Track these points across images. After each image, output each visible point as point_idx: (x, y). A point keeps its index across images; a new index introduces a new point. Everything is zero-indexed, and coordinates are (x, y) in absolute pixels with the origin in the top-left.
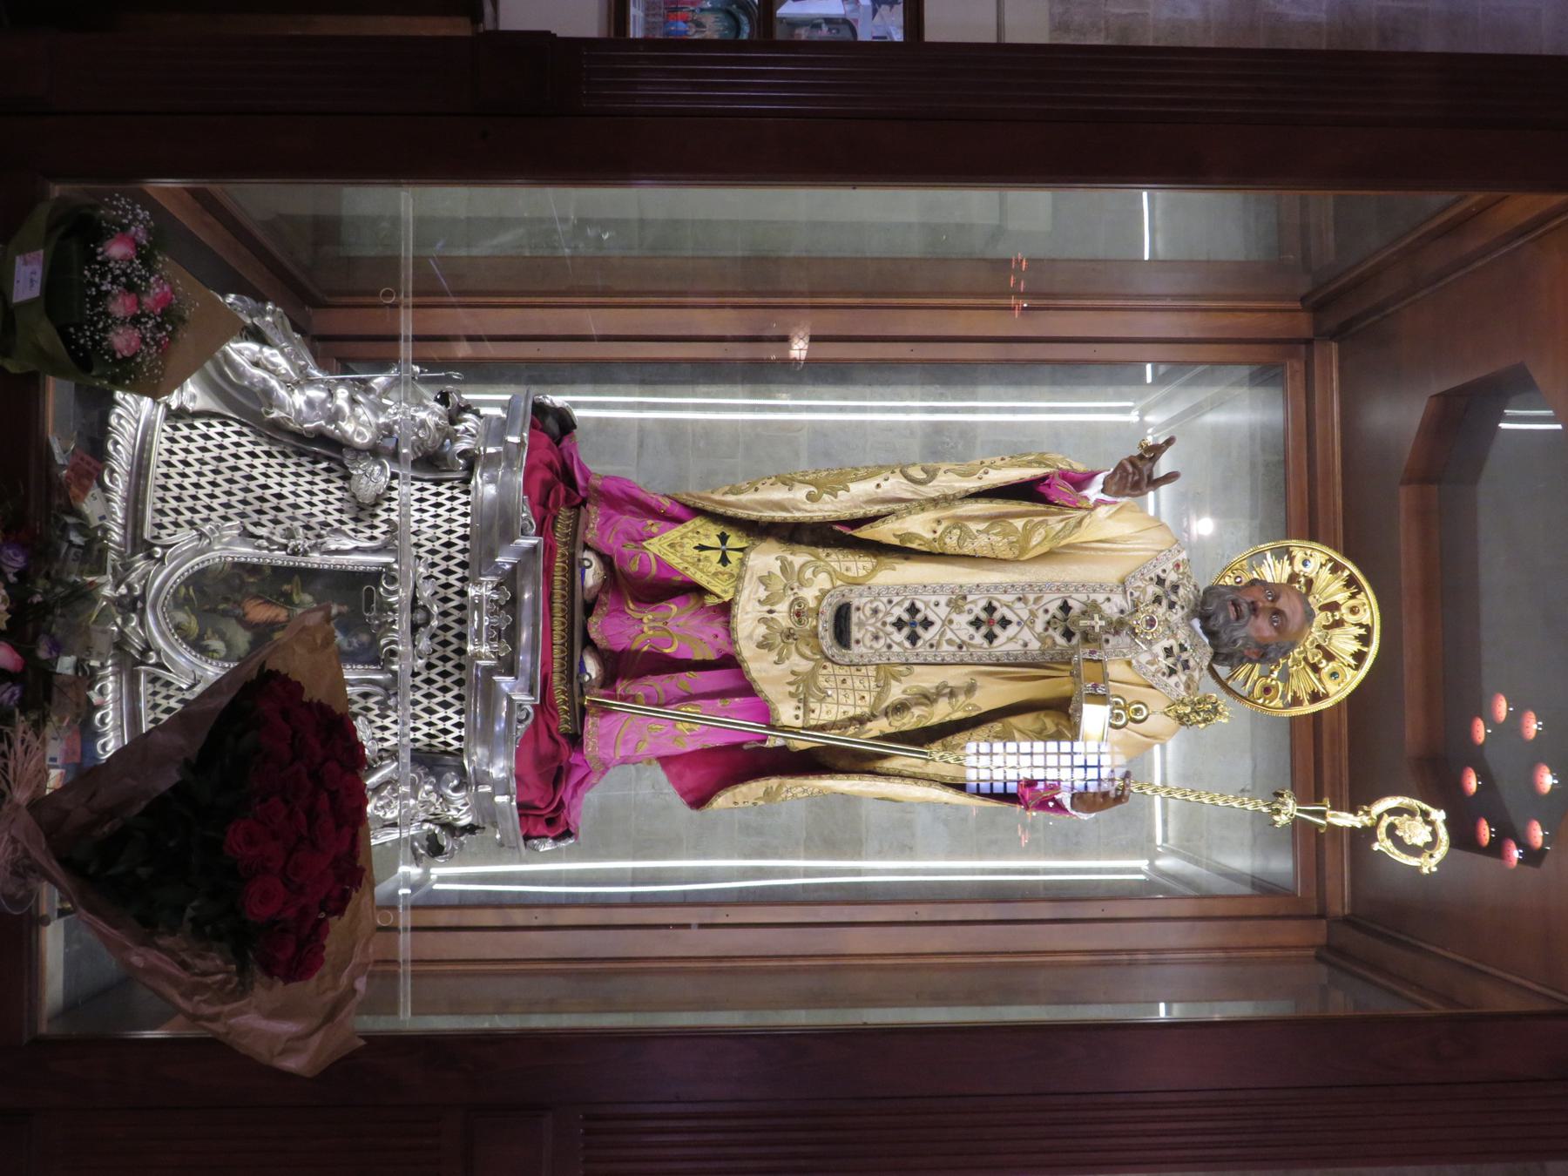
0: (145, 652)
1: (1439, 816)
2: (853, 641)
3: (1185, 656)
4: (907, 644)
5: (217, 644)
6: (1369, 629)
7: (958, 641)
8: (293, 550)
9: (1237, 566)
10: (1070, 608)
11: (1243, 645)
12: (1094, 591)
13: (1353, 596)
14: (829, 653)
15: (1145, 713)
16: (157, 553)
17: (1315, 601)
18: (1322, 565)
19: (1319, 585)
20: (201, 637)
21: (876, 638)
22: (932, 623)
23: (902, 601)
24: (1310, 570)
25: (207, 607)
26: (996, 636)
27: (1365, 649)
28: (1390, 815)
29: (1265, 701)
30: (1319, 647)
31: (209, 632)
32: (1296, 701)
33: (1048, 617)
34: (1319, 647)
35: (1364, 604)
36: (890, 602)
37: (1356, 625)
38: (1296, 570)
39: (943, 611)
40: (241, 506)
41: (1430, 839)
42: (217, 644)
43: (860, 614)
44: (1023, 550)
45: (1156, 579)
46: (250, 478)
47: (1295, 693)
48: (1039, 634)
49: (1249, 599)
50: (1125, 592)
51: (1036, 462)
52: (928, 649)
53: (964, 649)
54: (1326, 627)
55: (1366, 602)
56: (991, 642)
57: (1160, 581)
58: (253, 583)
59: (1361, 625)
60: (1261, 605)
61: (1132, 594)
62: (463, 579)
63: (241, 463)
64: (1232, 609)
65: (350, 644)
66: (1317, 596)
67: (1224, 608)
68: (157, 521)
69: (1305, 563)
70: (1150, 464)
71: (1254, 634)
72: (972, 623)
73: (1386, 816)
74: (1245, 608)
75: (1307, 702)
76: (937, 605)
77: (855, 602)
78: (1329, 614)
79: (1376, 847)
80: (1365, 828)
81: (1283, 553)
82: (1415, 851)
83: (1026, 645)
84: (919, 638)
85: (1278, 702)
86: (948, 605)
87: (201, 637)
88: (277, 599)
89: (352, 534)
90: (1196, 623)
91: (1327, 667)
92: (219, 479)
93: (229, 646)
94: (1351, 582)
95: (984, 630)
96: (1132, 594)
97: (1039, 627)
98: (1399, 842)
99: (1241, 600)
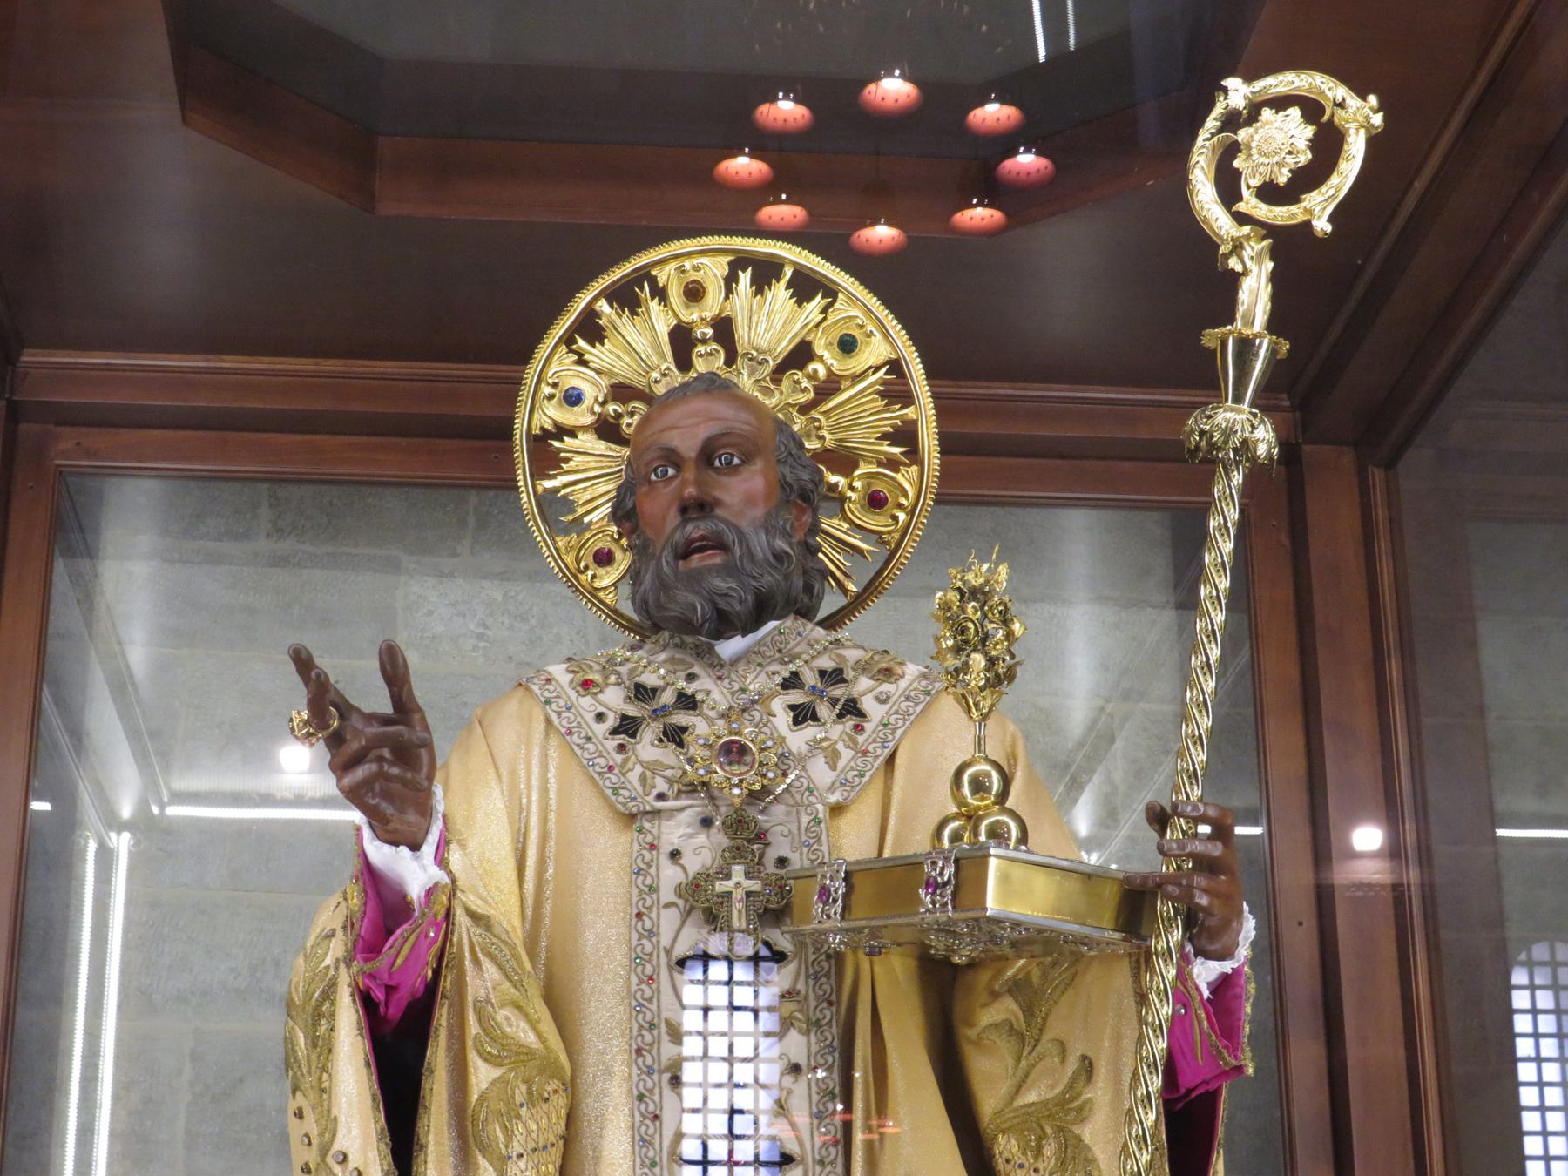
3: (810, 678)
6: (740, 262)
9: (569, 559)
11: (787, 535)
12: (653, 889)
13: (660, 294)
15: (987, 767)
17: (664, 376)
18: (582, 362)
19: (625, 369)
24: (592, 389)
27: (788, 272)
28: (1240, 198)
29: (900, 506)
32: (905, 435)
35: (682, 270)
37: (729, 291)
38: (589, 420)
44: (548, 1067)
47: (884, 436)
49: (673, 518)
50: (657, 813)
51: (315, 1024)
54: (730, 360)
55: (673, 265)
57: (627, 727)
59: (730, 280)
60: (691, 490)
61: (661, 797)
64: (696, 561)
66: (655, 375)
67: (695, 579)
70: (356, 722)
71: (759, 512)
73: (1241, 207)
74: (695, 530)
75: (910, 412)
79: (1322, 225)
80: (1274, 254)
81: (545, 455)
82: (1328, 144)
85: (906, 478)
90: (729, 647)
94: (626, 297)
96: (661, 797)
99: (678, 537)
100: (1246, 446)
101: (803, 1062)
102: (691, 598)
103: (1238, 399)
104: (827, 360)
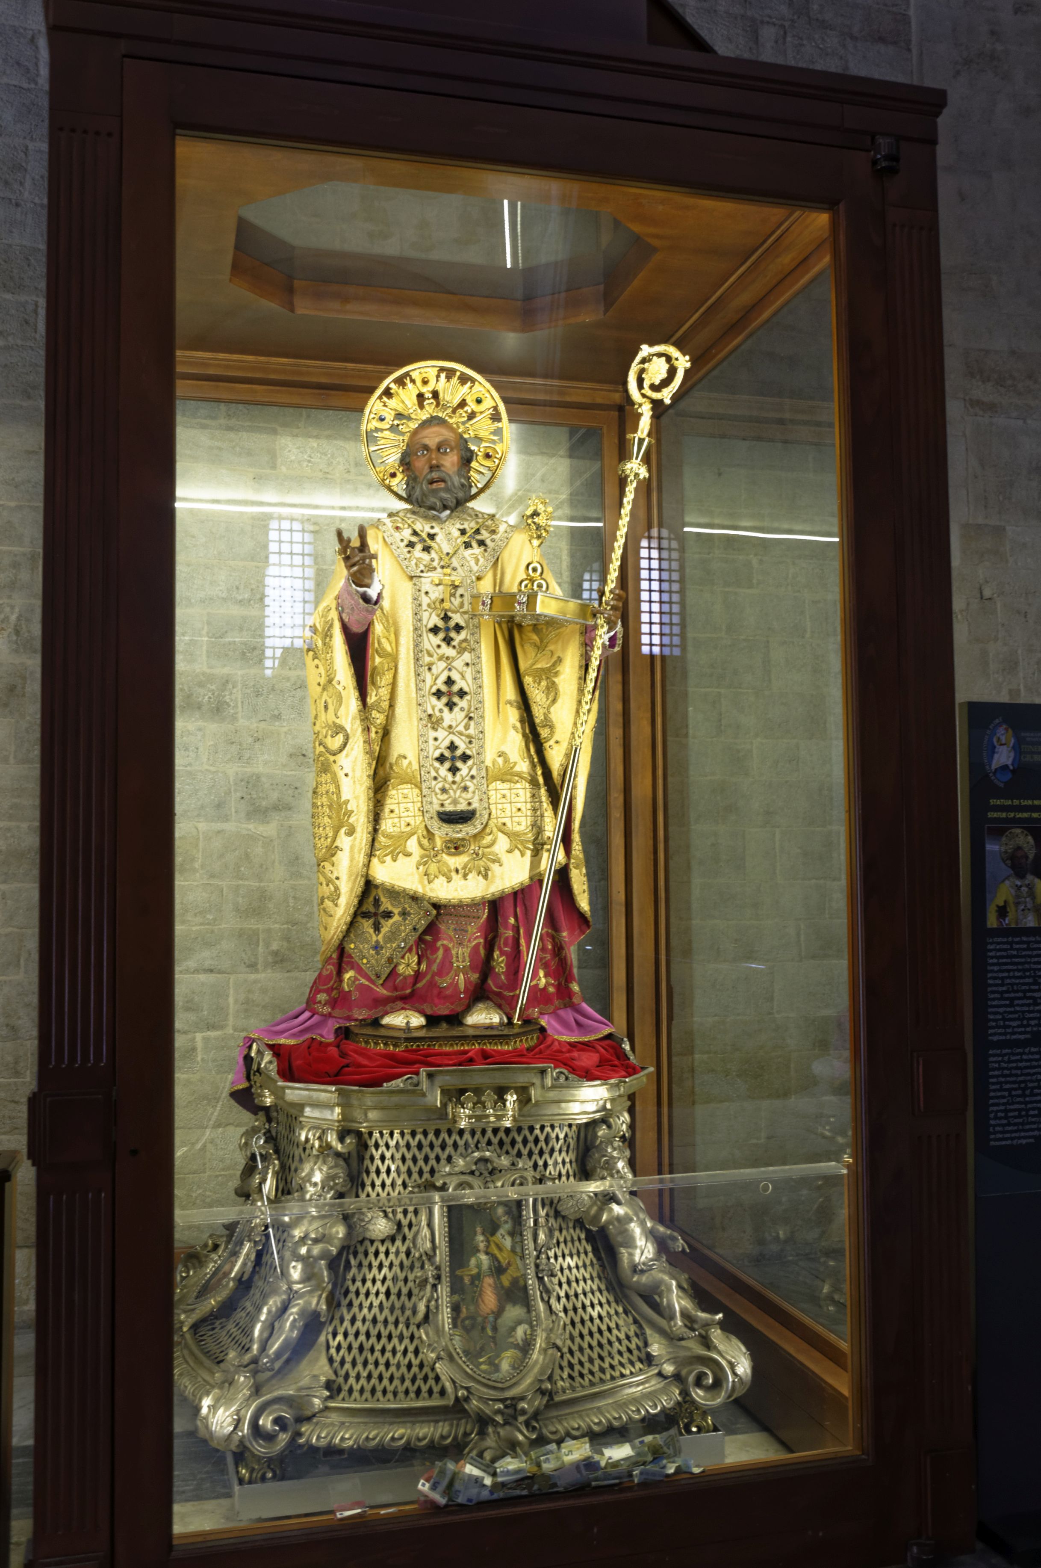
0: (543, 1392)
1: (645, 350)
2: (470, 808)
4: (470, 762)
5: (520, 1331)
7: (467, 720)
8: (436, 1279)
10: (436, 626)
12: (420, 605)
14: (480, 827)
16: (463, 1394)
19: (400, 408)
20: (516, 1346)
21: (465, 789)
22: (452, 743)
23: (435, 768)
25: (492, 1345)
26: (461, 689)
27: (458, 374)
30: (454, 412)
31: (511, 1340)
33: (443, 645)
34: (454, 412)
36: (435, 778)
37: (437, 381)
39: (441, 734)
40: (401, 1326)
41: (663, 359)
42: (520, 1331)
43: (446, 803)
45: (409, 549)
46: (374, 1321)
48: (458, 653)
49: (426, 470)
50: (420, 577)
52: (473, 745)
53: (472, 715)
54: (438, 405)
56: (466, 693)
57: (411, 545)
58: (467, 1309)
59: (438, 376)
61: (422, 571)
62: (450, 1132)
63: (363, 1330)
64: (434, 486)
65: (506, 1222)
68: (426, 1395)
69: (382, 419)
71: (456, 469)
72: (451, 709)
74: (435, 475)
76: (436, 739)
77: (437, 807)
78: (427, 402)
79: (668, 401)
80: (653, 409)
82: (672, 372)
83: (467, 664)
84: (464, 753)
86: (436, 730)
87: (516, 1346)
88: (477, 1286)
89: (414, 1229)
91: (472, 406)
92: (378, 1347)
93: (519, 1323)
95: (456, 699)
96: (422, 571)
97: (450, 652)
98: (666, 383)
100: (637, 475)
101: (469, 662)
102: (434, 500)
103: (637, 458)
104: (472, 406)
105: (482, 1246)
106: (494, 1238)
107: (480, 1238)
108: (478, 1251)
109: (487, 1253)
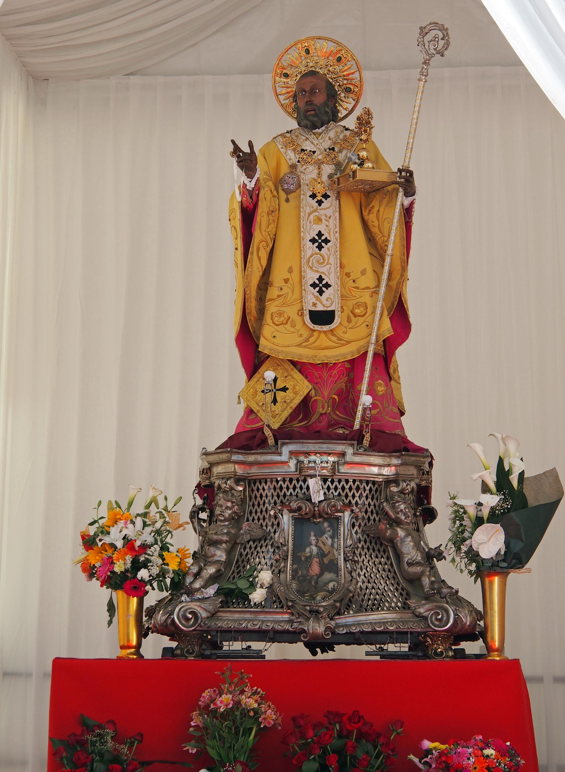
31: (325, 588)
60: (308, 99)
74: (310, 107)
88: (309, 562)
93: (331, 581)
105: (314, 542)
106: (321, 539)
107: (313, 538)
108: (312, 545)
109: (316, 546)
